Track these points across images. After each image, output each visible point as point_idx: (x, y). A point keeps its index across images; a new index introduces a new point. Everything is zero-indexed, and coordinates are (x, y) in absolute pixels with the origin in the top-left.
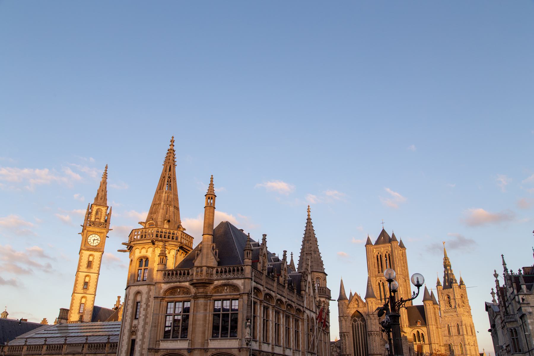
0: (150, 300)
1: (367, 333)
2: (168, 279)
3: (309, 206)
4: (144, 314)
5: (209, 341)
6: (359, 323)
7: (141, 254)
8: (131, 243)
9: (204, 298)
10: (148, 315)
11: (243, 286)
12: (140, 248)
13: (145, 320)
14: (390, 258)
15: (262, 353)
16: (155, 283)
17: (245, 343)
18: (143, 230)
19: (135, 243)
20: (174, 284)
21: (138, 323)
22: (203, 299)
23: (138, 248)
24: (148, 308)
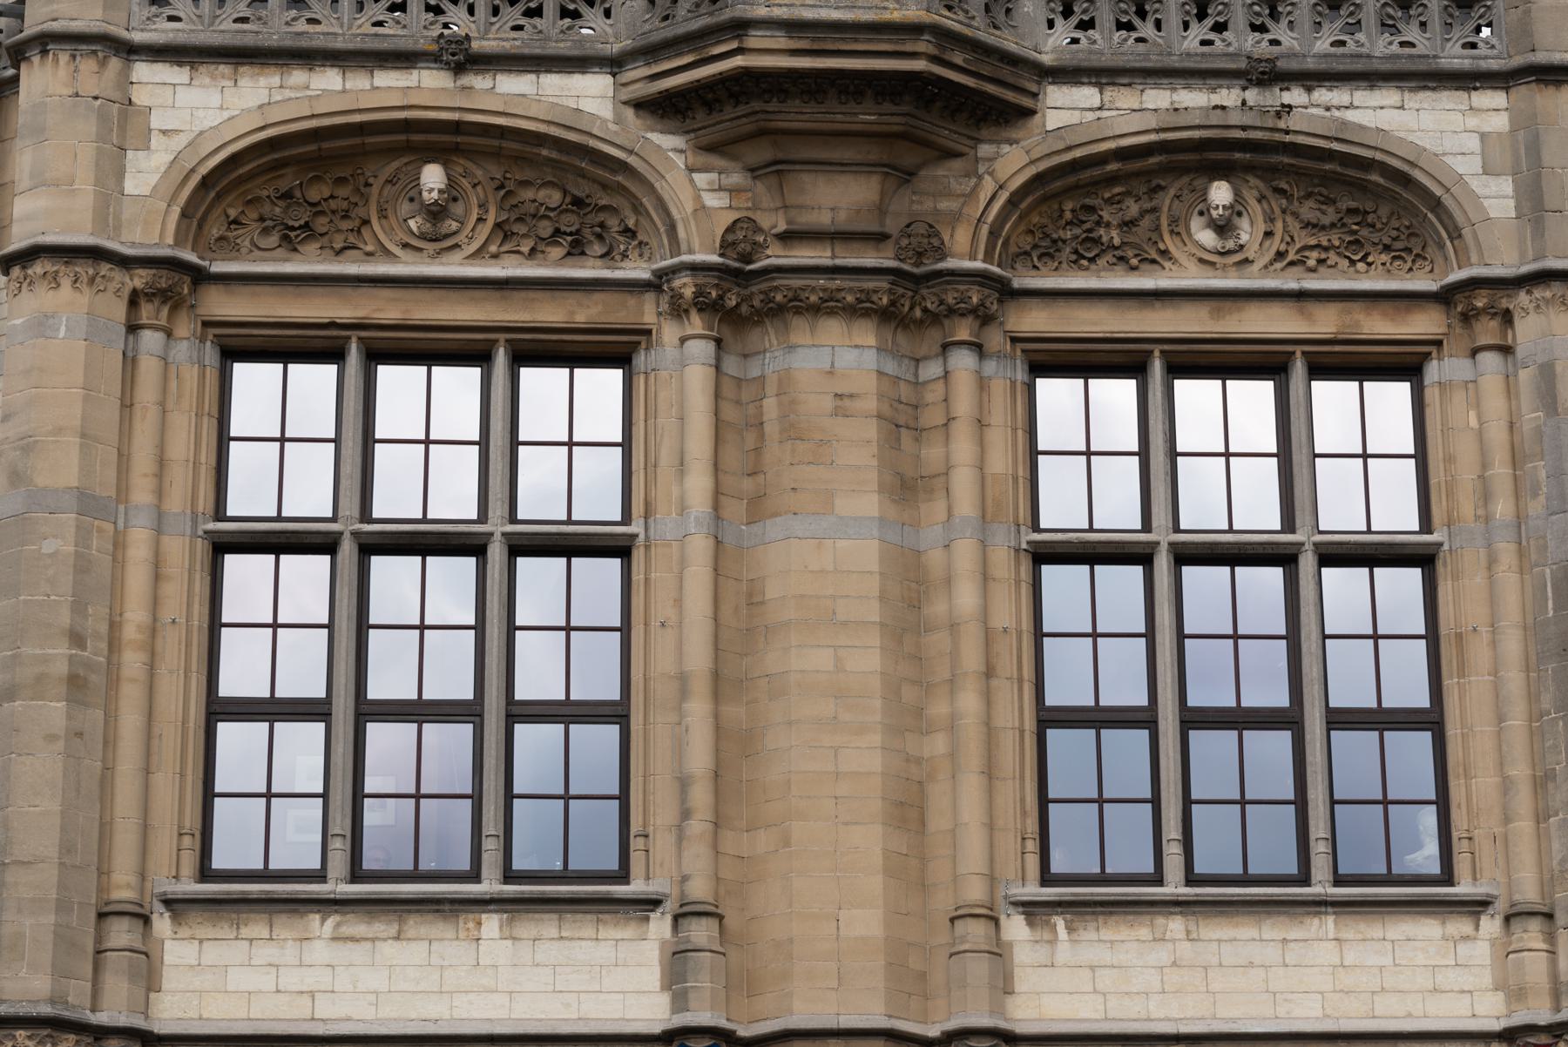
5: (1016, 928)
9: (888, 316)
11: (1506, 185)
20: (359, 81)
22: (867, 334)
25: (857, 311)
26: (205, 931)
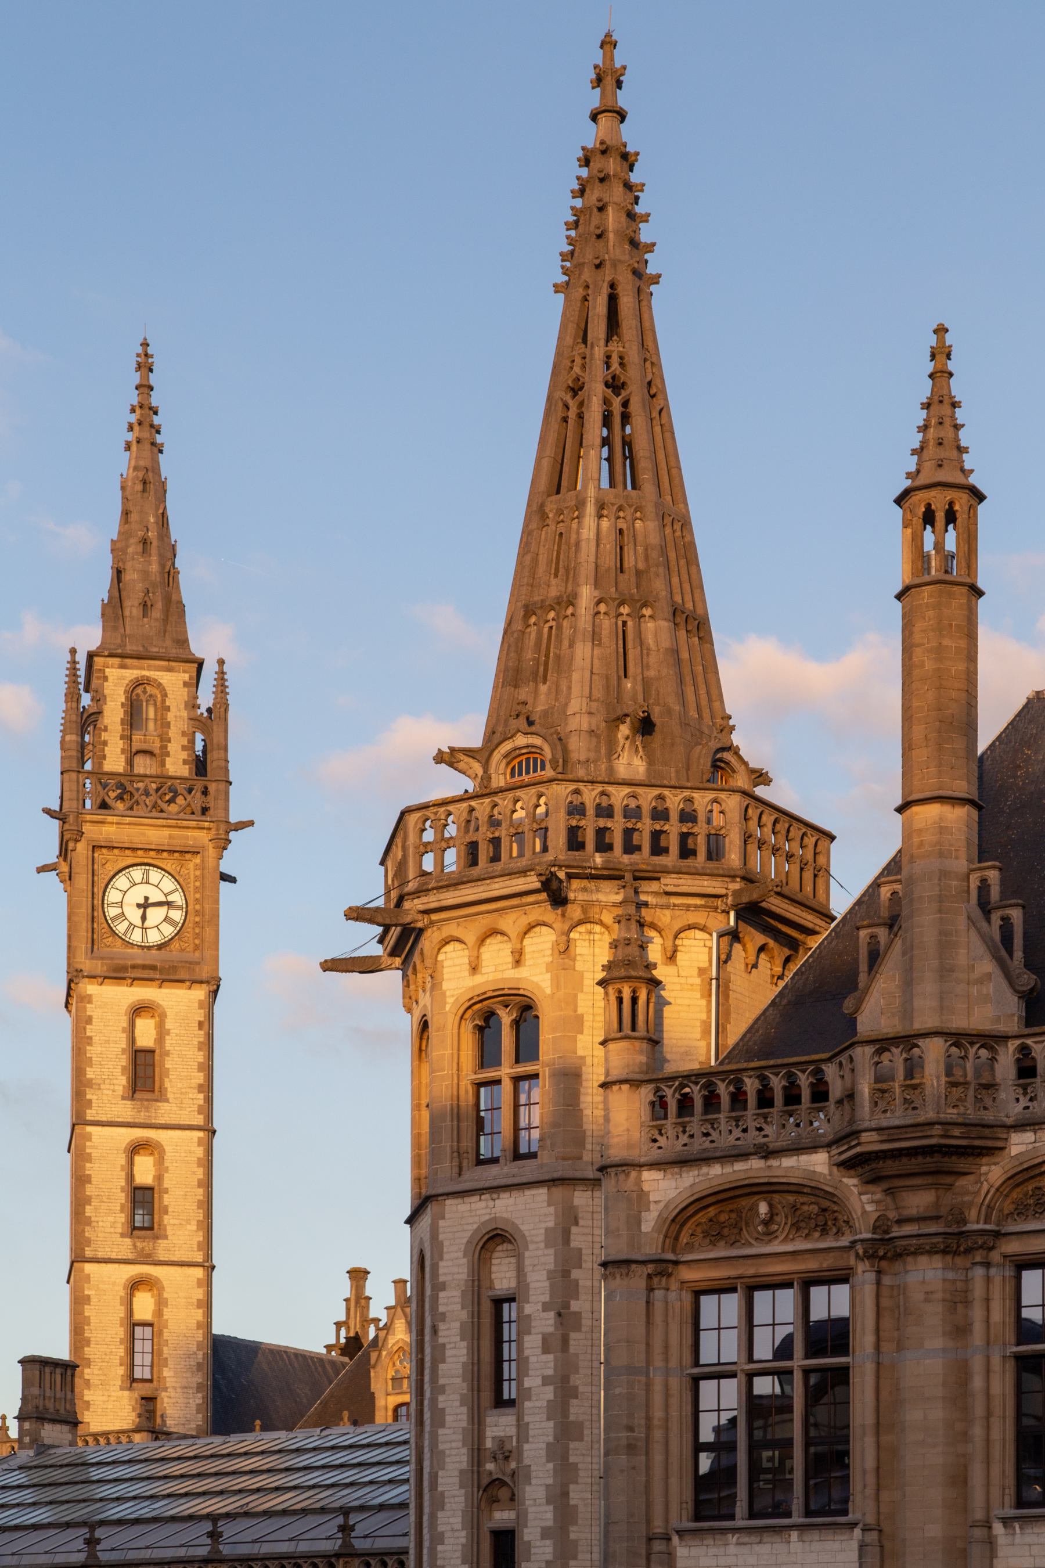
0: (577, 1281)
2: (684, 1139)
4: (550, 1372)
7: (479, 979)
8: (407, 905)
9: (945, 1252)
10: (576, 1380)
12: (471, 938)
13: (559, 1409)
16: (602, 1169)
18: (472, 810)
19: (432, 900)
20: (728, 1169)
21: (518, 1426)
22: (937, 1261)
23: (459, 940)
24: (573, 1335)
25: (931, 1252)
26: (690, 1543)
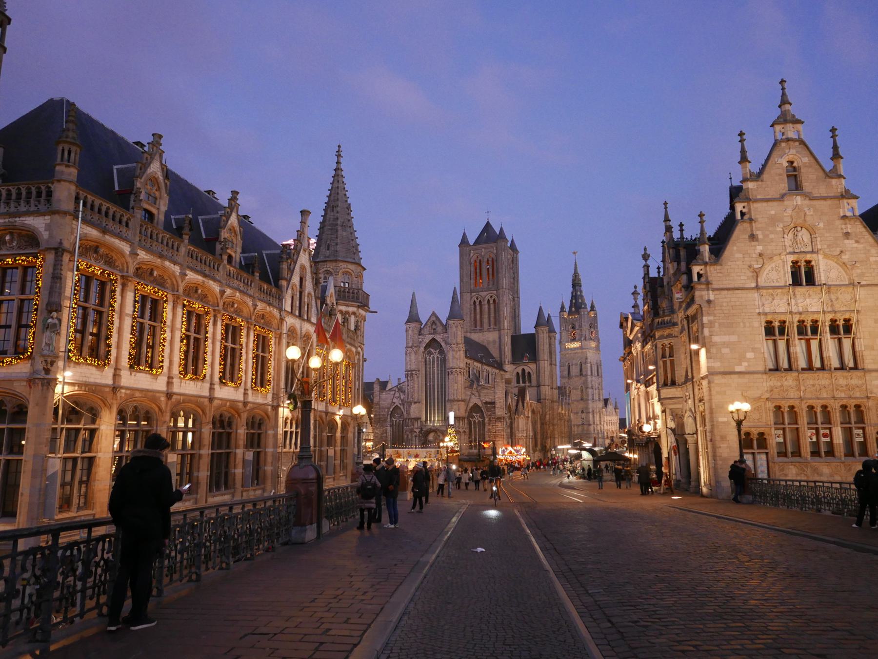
1: (447, 371)
3: (339, 146)
6: (436, 357)
11: (47, 233)
14: (494, 262)
15: (123, 391)
17: (40, 366)
